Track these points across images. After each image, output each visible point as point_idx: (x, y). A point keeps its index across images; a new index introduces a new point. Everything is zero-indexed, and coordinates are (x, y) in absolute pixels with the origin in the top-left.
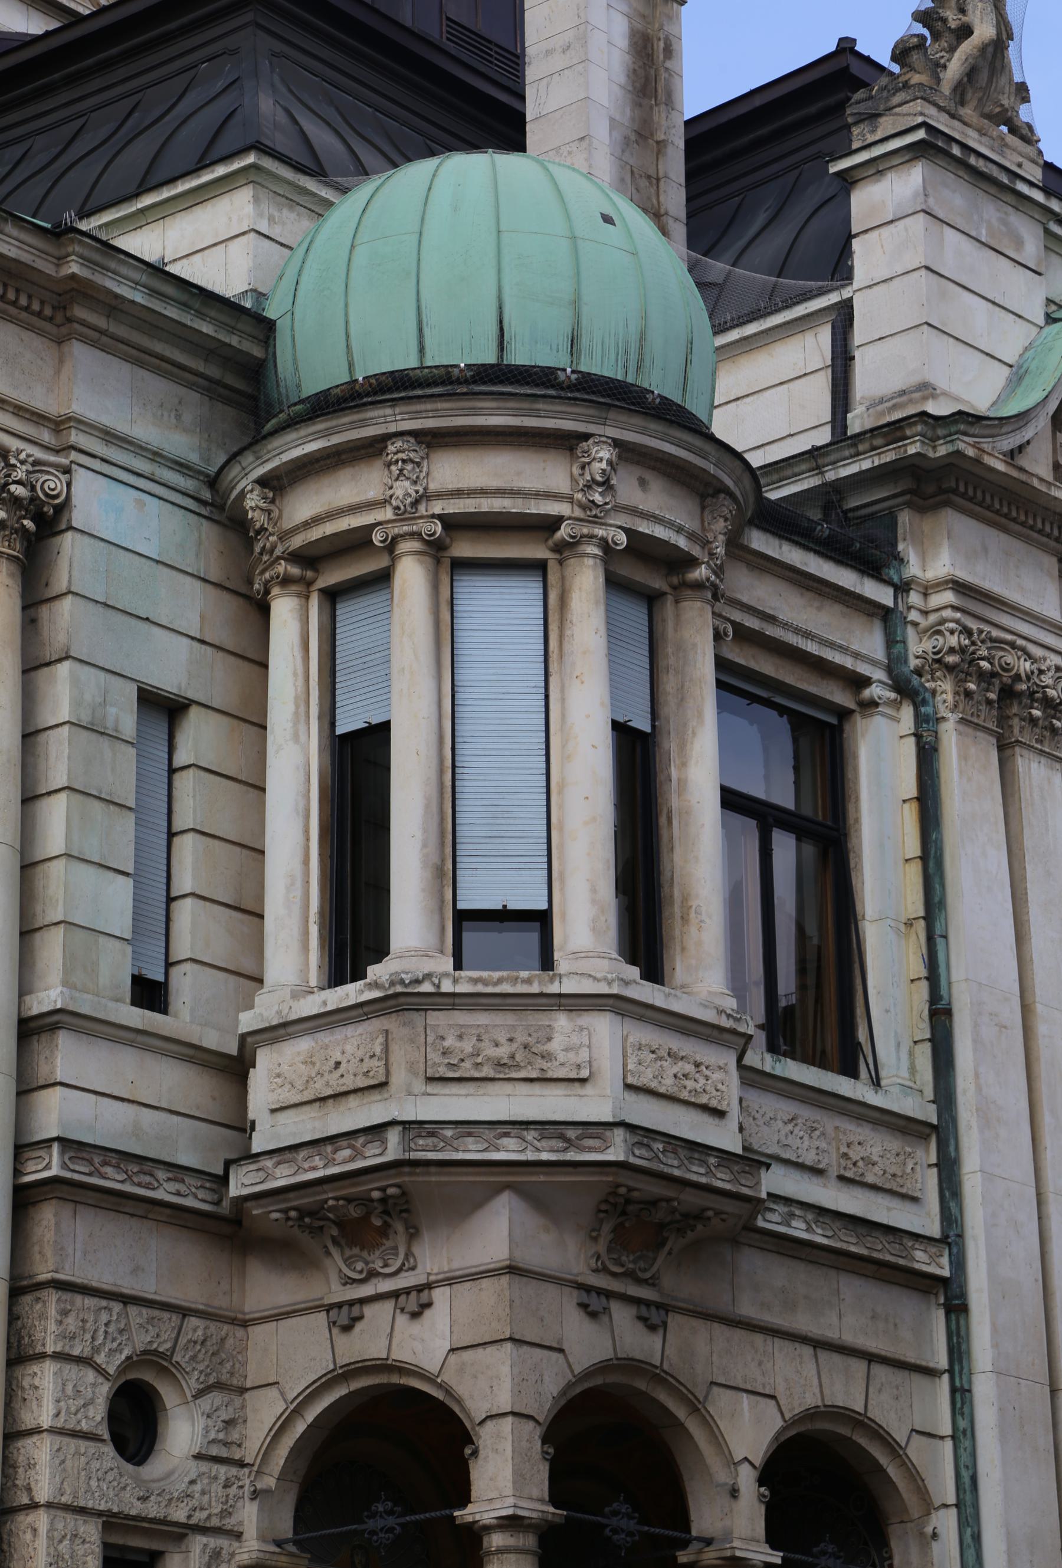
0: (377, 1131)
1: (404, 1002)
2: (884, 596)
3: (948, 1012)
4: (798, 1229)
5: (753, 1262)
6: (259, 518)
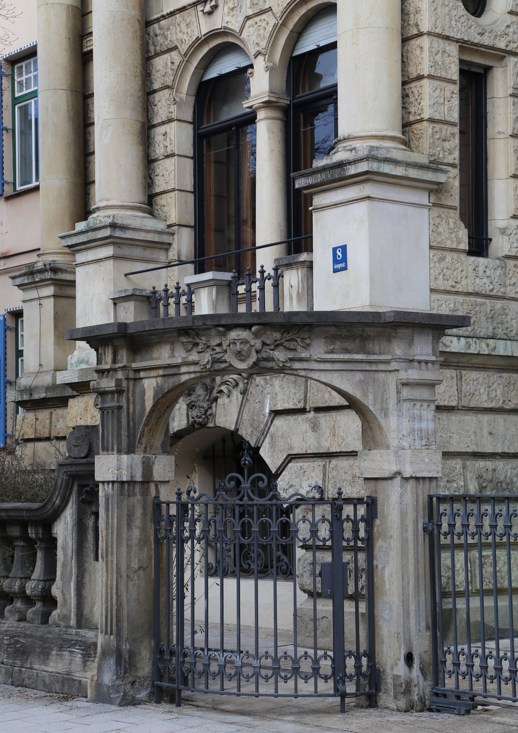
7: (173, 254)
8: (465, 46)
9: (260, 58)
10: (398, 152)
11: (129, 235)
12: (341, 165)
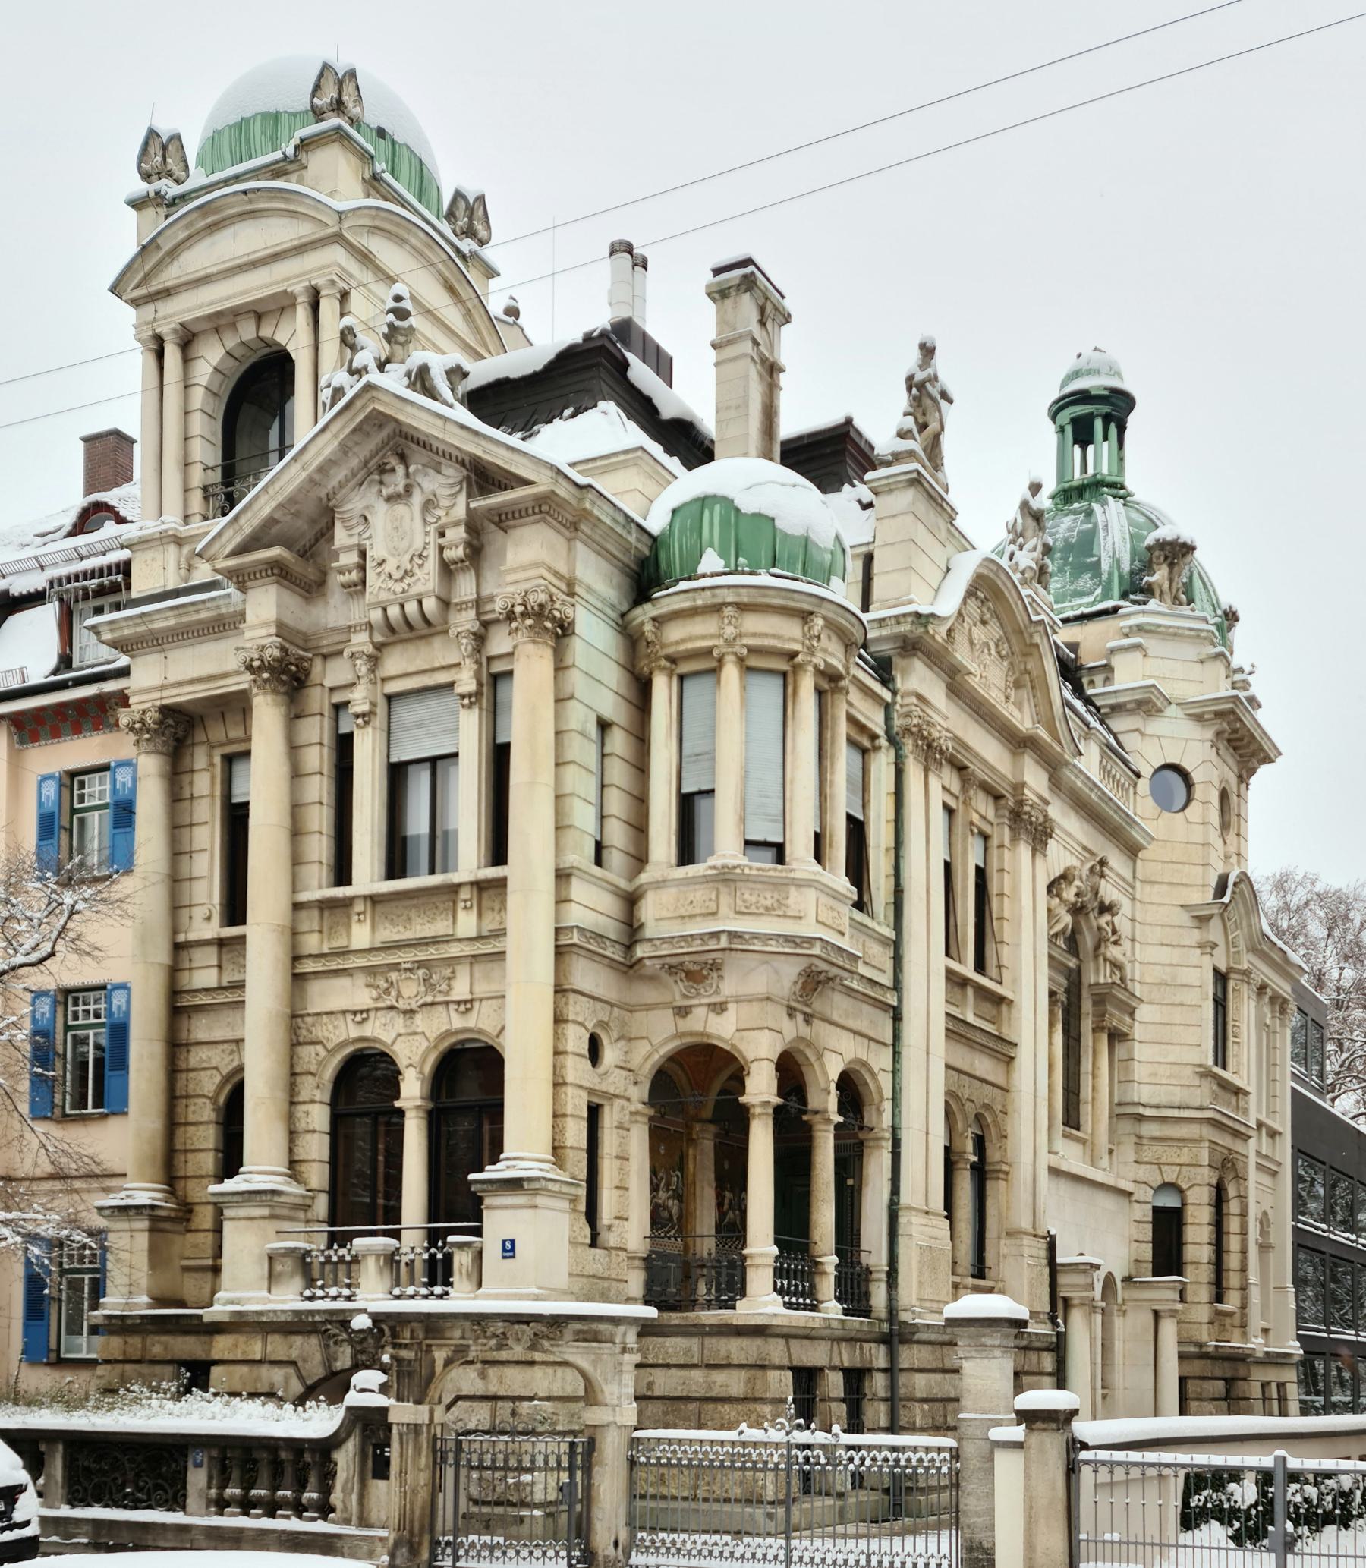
0: (715, 935)
1: (726, 878)
2: (887, 695)
3: (902, 891)
6: (651, 637)
7: (310, 1215)
8: (591, 1092)
9: (412, 1069)
11: (282, 1199)
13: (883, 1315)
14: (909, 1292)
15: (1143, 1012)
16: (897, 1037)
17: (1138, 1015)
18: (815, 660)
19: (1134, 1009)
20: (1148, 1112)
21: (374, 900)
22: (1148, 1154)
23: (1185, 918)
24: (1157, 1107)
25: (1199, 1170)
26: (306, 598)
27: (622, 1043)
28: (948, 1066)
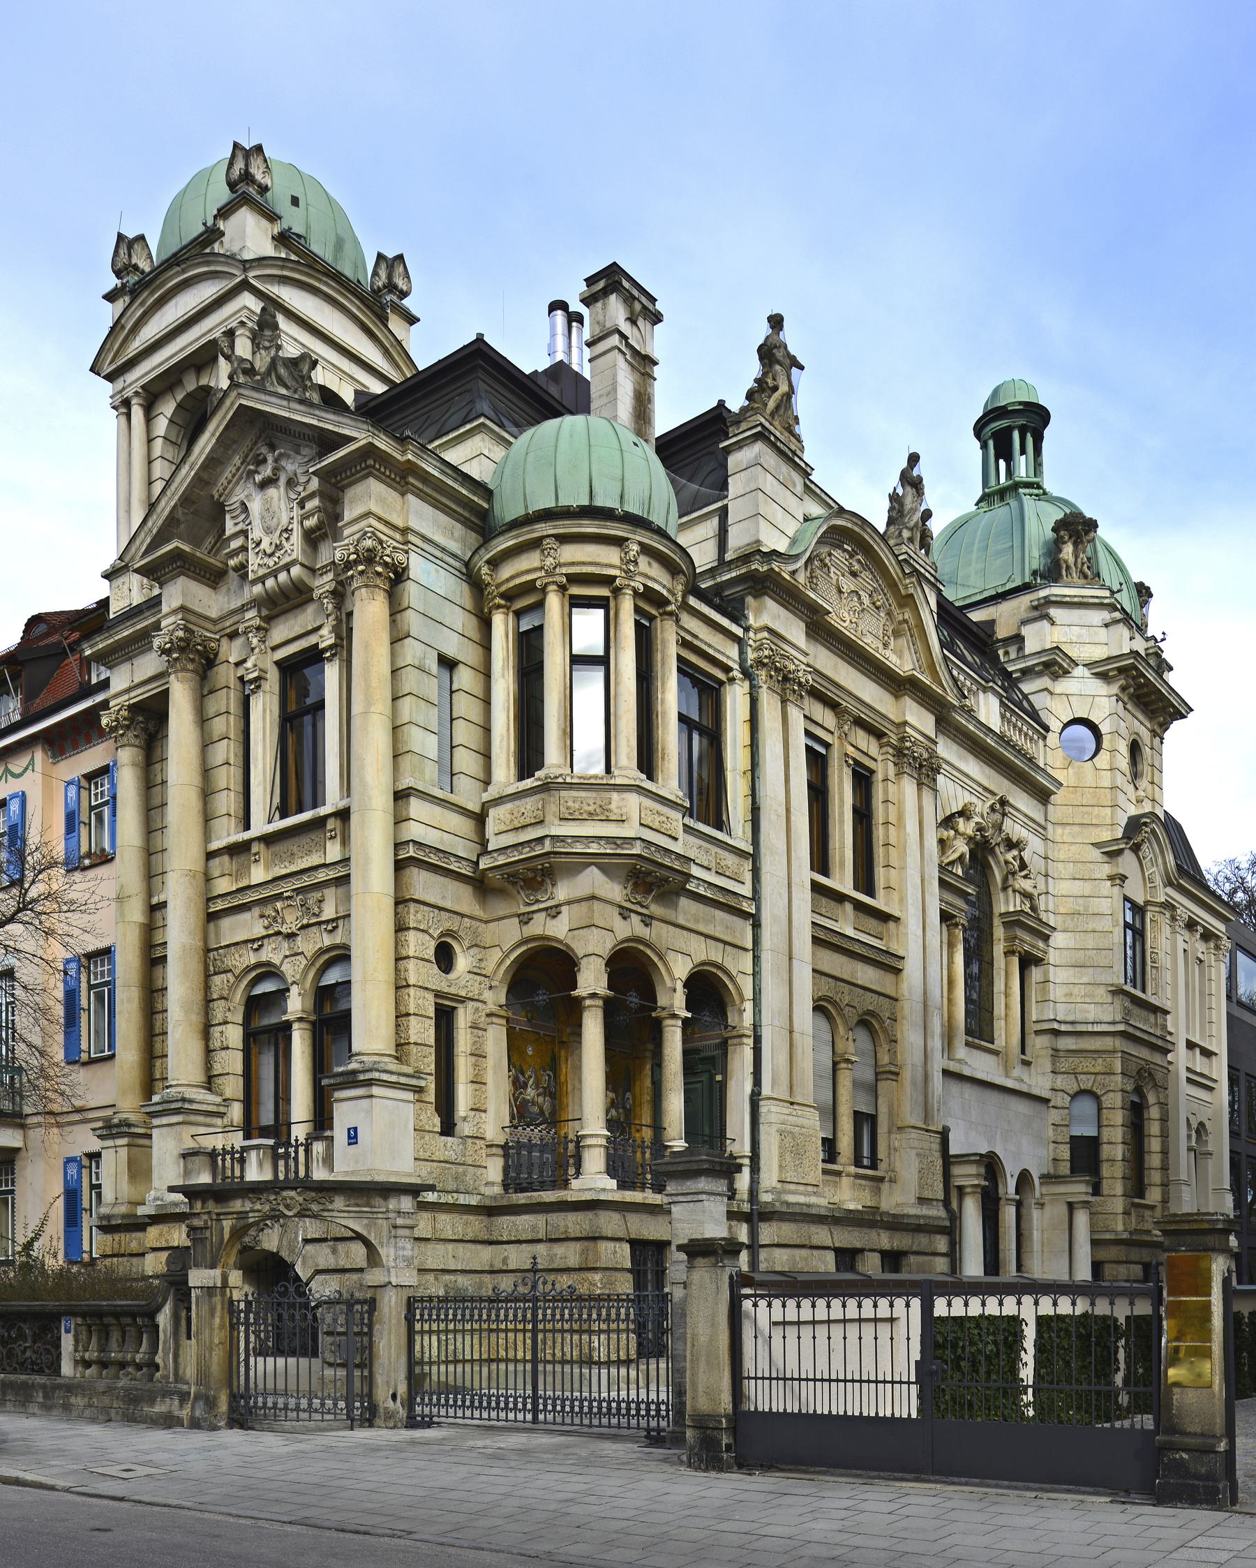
2: (739, 631)
4: (701, 891)
5: (684, 902)
10: (393, 1066)
12: (354, 1072)
13: (746, 1197)
14: (769, 1177)
15: (1058, 939)
16: (756, 941)
17: (1051, 942)
18: (632, 584)
19: (1049, 936)
20: (1063, 1028)
21: (268, 840)
22: (1064, 1065)
23: (1096, 854)
24: (1073, 1023)
25: (1112, 1077)
26: (215, 589)
27: (475, 950)
28: (814, 970)
